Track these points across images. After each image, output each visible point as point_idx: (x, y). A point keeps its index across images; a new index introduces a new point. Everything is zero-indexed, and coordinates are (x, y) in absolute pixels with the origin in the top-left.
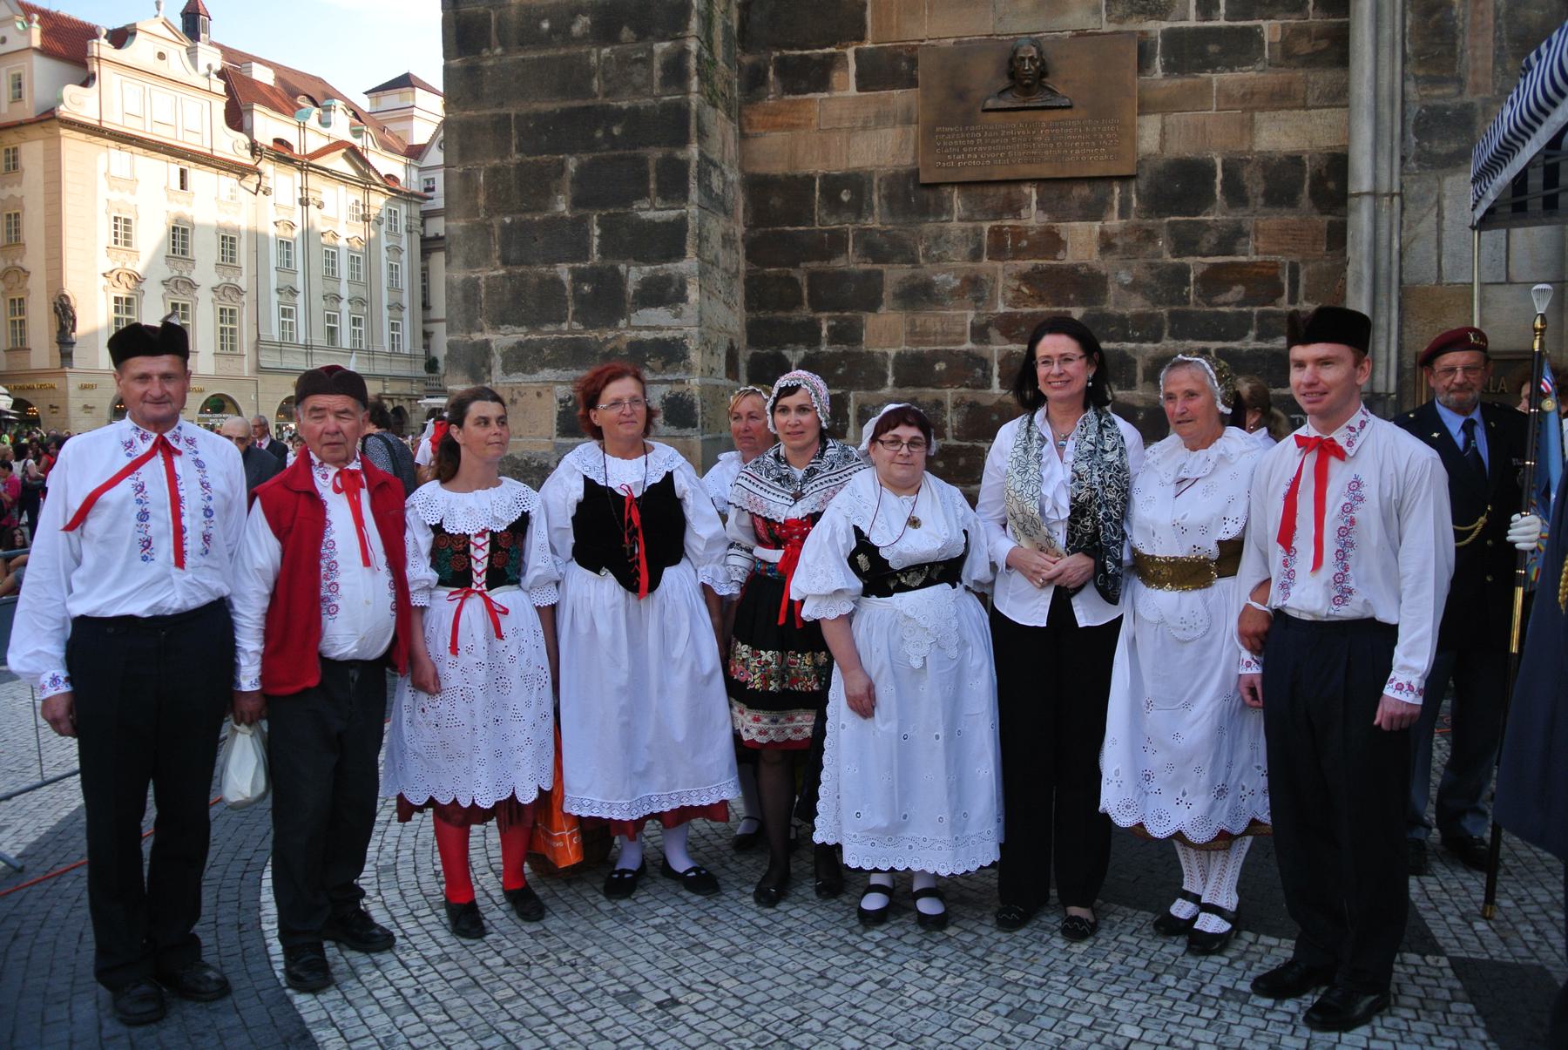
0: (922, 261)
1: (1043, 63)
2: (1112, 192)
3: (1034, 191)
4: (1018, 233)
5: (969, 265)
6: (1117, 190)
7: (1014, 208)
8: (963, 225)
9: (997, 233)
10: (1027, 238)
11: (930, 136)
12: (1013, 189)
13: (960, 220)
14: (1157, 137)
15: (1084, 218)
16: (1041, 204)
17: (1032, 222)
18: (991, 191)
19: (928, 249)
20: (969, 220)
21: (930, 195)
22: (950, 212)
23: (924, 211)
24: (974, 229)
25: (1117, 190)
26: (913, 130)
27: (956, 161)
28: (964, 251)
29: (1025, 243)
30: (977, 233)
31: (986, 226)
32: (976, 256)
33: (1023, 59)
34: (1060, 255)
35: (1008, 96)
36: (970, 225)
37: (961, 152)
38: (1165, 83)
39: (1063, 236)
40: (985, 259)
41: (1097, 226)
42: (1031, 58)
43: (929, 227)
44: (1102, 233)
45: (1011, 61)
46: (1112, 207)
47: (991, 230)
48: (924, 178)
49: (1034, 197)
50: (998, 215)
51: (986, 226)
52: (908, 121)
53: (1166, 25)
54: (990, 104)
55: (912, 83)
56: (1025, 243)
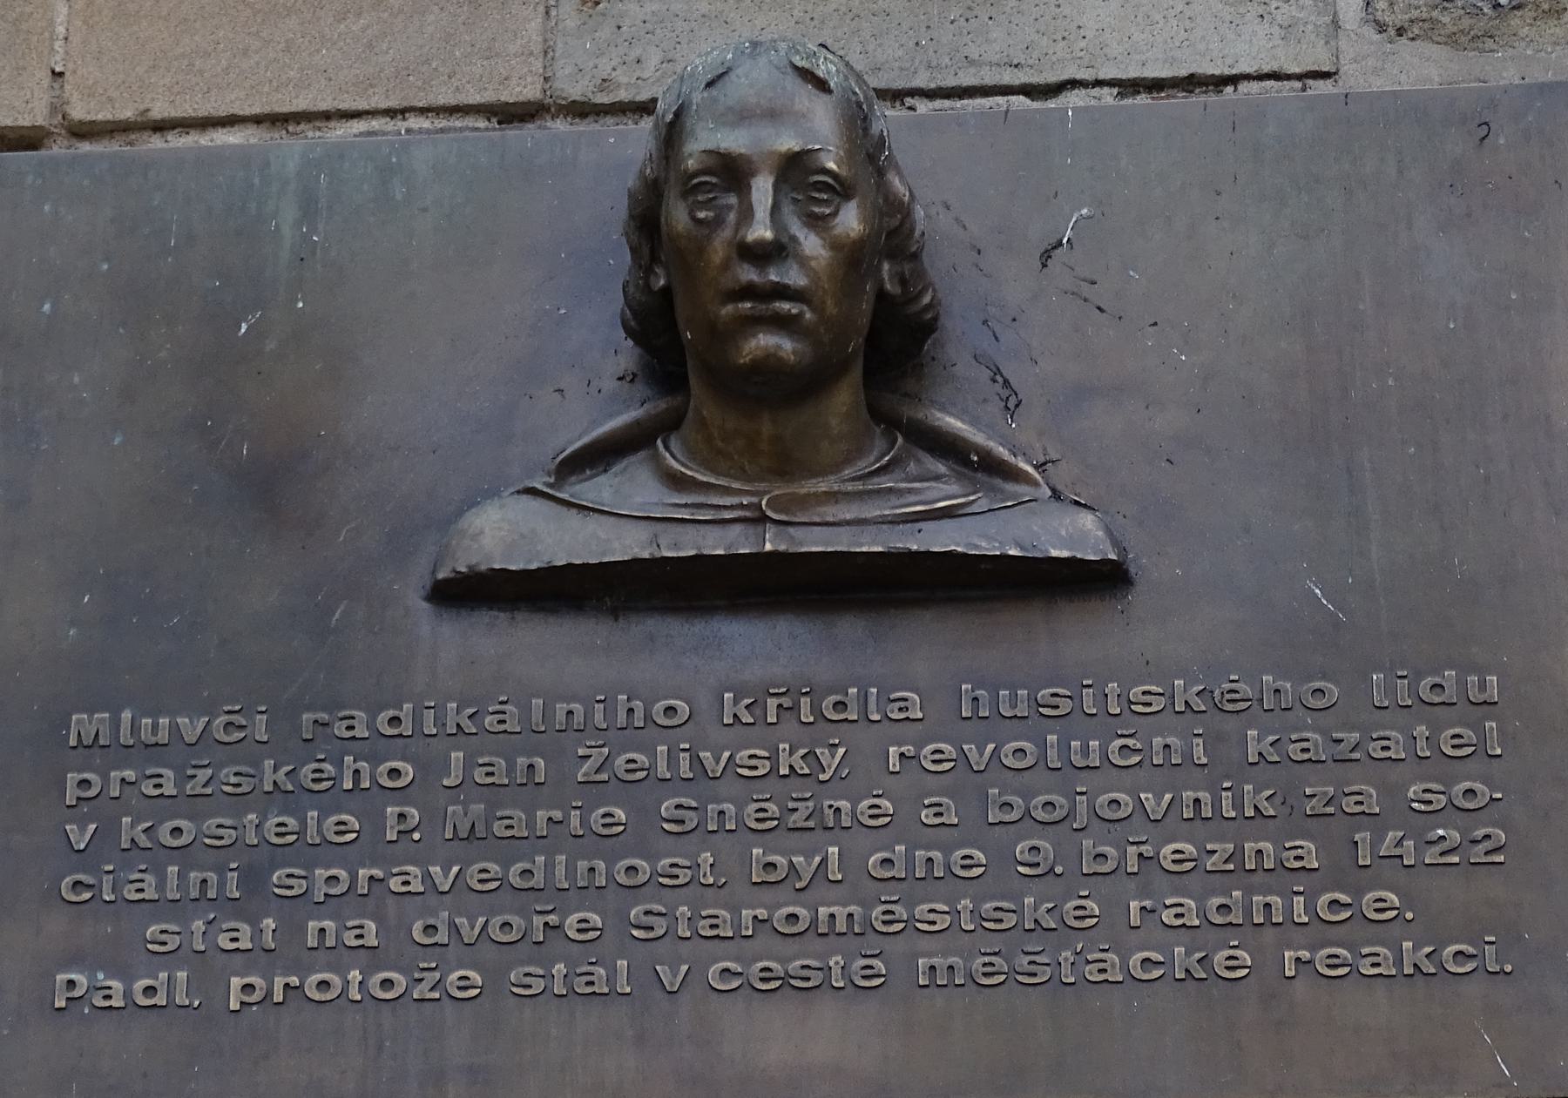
1: (895, 235)
27: (208, 967)
33: (732, 172)
35: (632, 487)
37: (255, 895)
42: (795, 169)
45: (646, 222)
54: (510, 531)
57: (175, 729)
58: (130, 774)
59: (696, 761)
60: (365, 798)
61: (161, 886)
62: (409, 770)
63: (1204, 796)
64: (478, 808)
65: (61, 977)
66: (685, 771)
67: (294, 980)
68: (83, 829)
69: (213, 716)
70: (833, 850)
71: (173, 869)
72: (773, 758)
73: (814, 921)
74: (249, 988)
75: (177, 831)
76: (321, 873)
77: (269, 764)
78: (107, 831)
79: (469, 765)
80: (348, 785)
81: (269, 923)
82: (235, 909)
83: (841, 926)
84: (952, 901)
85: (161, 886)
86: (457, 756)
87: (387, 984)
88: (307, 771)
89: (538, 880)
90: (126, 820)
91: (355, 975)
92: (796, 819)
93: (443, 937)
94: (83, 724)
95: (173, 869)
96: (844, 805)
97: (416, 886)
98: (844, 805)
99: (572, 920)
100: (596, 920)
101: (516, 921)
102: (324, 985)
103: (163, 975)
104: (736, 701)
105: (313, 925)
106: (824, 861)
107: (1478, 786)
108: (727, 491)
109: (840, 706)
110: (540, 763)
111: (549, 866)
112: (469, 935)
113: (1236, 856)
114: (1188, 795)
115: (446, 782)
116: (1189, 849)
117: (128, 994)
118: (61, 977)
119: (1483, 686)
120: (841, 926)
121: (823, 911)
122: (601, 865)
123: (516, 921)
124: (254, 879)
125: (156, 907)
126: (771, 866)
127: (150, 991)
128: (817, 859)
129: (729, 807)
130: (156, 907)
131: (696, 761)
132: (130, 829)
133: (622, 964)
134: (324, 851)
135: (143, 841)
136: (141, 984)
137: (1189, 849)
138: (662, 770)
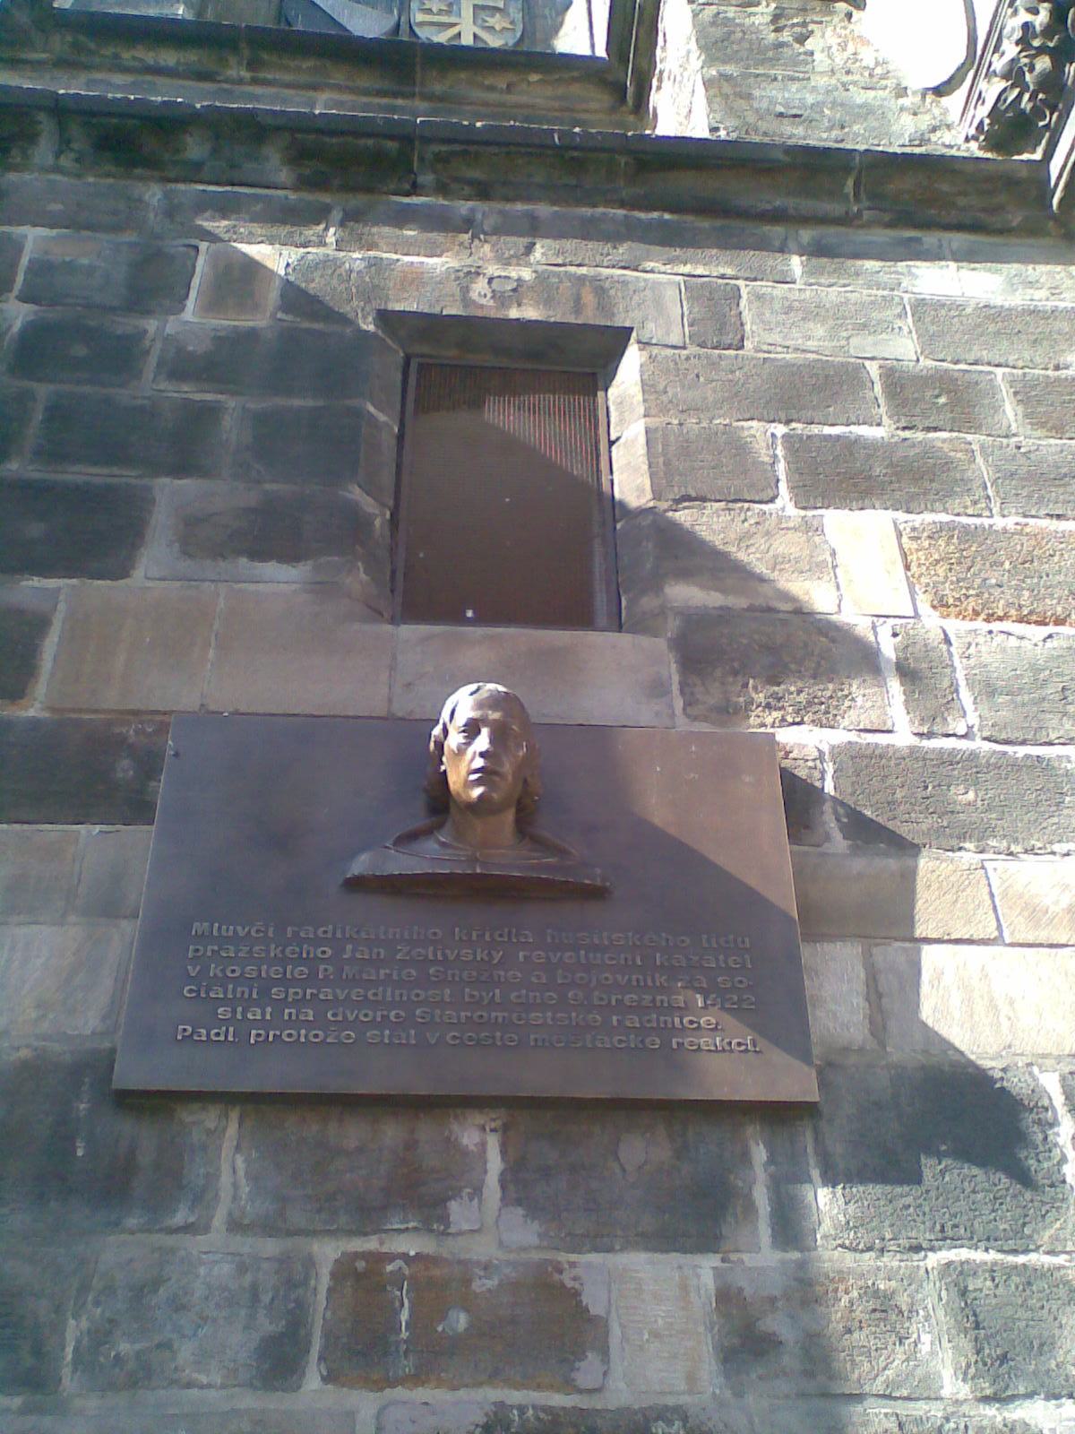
0: (69, 1381)
2: (745, 1157)
3: (493, 1143)
4: (437, 1285)
5: (249, 1401)
6: (760, 1154)
7: (422, 1193)
8: (246, 1245)
9: (364, 1279)
10: (467, 1304)
11: (171, 948)
12: (426, 1131)
13: (236, 1226)
14: (859, 1001)
15: (664, 1240)
16: (518, 1185)
17: (482, 1249)
18: (351, 1132)
19: (100, 1336)
20: (268, 1227)
21: (144, 1137)
22: (202, 1197)
23: (114, 1187)
24: (284, 1261)
25: (760, 1154)
26: (123, 936)
28: (240, 1341)
29: (460, 1321)
30: (294, 1276)
31: (328, 1252)
32: (278, 1363)
34: (588, 1371)
36: (271, 1247)
38: (858, 865)
39: (594, 1299)
40: (313, 1380)
41: (706, 1268)
43: (120, 1249)
44: (726, 1297)
46: (750, 1208)
47: (345, 1271)
48: (132, 1074)
49: (495, 1163)
50: (368, 1216)
51: (328, 1252)
52: (107, 907)
53: (838, 737)
55: (138, 809)
56: (460, 1321)
57: (235, 931)
58: (216, 948)
59: (444, 955)
61: (225, 993)
62: (329, 952)
63: (641, 977)
65: (181, 1027)
66: (440, 957)
67: (278, 1033)
68: (194, 969)
70: (497, 991)
71: (231, 986)
72: (475, 954)
73: (490, 1019)
74: (259, 1035)
75: (233, 971)
76: (291, 991)
77: (273, 946)
78: (206, 969)
79: (354, 951)
80: (304, 955)
81: (269, 1010)
82: (257, 1003)
83: (500, 1020)
85: (225, 993)
86: (349, 947)
87: (316, 1036)
88: (288, 950)
89: (380, 998)
90: (213, 966)
91: (303, 1032)
92: (483, 978)
93: (340, 1018)
94: (198, 927)
95: (231, 986)
96: (502, 973)
97: (330, 997)
98: (502, 973)
99: (393, 1013)
100: (403, 1014)
101: (370, 1013)
102: (290, 1035)
103: (224, 1028)
104: (460, 931)
105: (287, 1011)
107: (744, 980)
108: (461, 849)
109: (501, 936)
110: (382, 951)
111: (385, 992)
112: (351, 1018)
113: (654, 1001)
114: (634, 977)
115: (345, 957)
116: (635, 997)
117: (208, 1035)
118: (181, 1027)
119: (743, 942)
120: (500, 1020)
122: (404, 992)
123: (370, 1013)
125: (224, 1001)
126: (472, 996)
127: (218, 1034)
128: (491, 994)
129: (457, 972)
130: (224, 1001)
133: (413, 1032)
134: (294, 981)
135: (220, 975)
136: (213, 1032)
137: (635, 997)
138: (431, 957)
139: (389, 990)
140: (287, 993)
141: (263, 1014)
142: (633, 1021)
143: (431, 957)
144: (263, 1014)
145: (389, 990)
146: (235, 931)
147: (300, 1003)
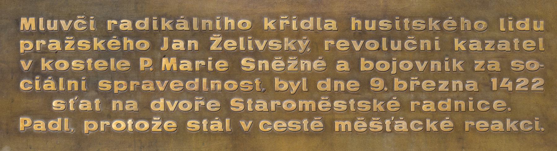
57: (60, 26)
59: (254, 45)
60: (133, 56)
64: (173, 60)
66: (250, 48)
69: (74, 20)
76: (116, 83)
78: (37, 64)
84: (347, 101)
106: (301, 83)
113: (450, 86)
121: (301, 103)
124: (93, 84)
128: (299, 83)
131: (254, 45)
132: (45, 65)
138: (242, 48)
139: (205, 80)
140: (112, 84)
141: (93, 105)
142: (428, 106)
143: (242, 48)
144: (93, 105)
145: (205, 80)
146: (60, 26)
147: (125, 95)
